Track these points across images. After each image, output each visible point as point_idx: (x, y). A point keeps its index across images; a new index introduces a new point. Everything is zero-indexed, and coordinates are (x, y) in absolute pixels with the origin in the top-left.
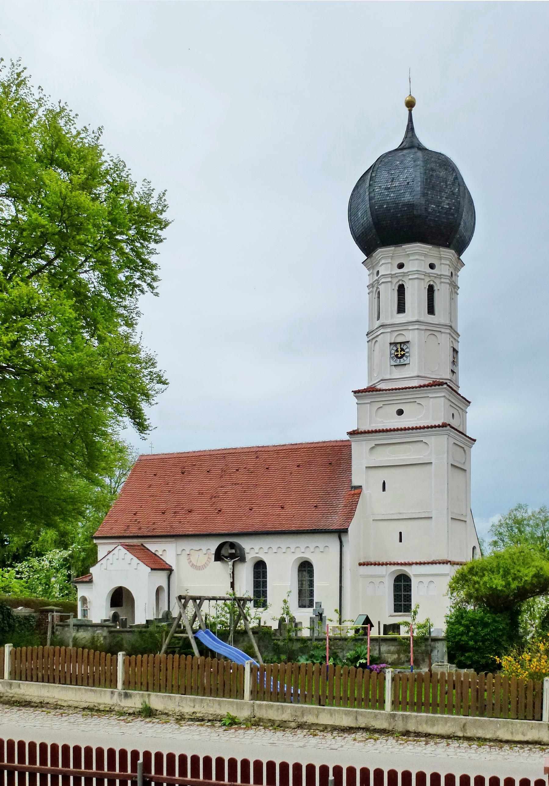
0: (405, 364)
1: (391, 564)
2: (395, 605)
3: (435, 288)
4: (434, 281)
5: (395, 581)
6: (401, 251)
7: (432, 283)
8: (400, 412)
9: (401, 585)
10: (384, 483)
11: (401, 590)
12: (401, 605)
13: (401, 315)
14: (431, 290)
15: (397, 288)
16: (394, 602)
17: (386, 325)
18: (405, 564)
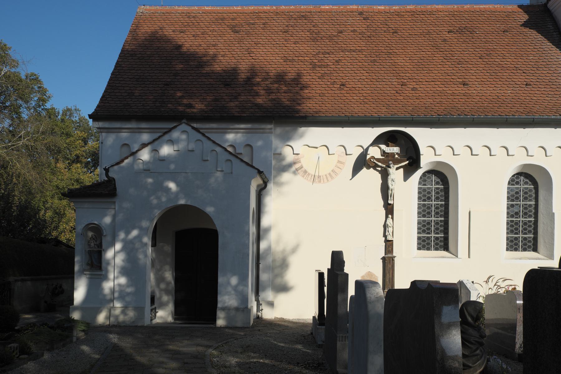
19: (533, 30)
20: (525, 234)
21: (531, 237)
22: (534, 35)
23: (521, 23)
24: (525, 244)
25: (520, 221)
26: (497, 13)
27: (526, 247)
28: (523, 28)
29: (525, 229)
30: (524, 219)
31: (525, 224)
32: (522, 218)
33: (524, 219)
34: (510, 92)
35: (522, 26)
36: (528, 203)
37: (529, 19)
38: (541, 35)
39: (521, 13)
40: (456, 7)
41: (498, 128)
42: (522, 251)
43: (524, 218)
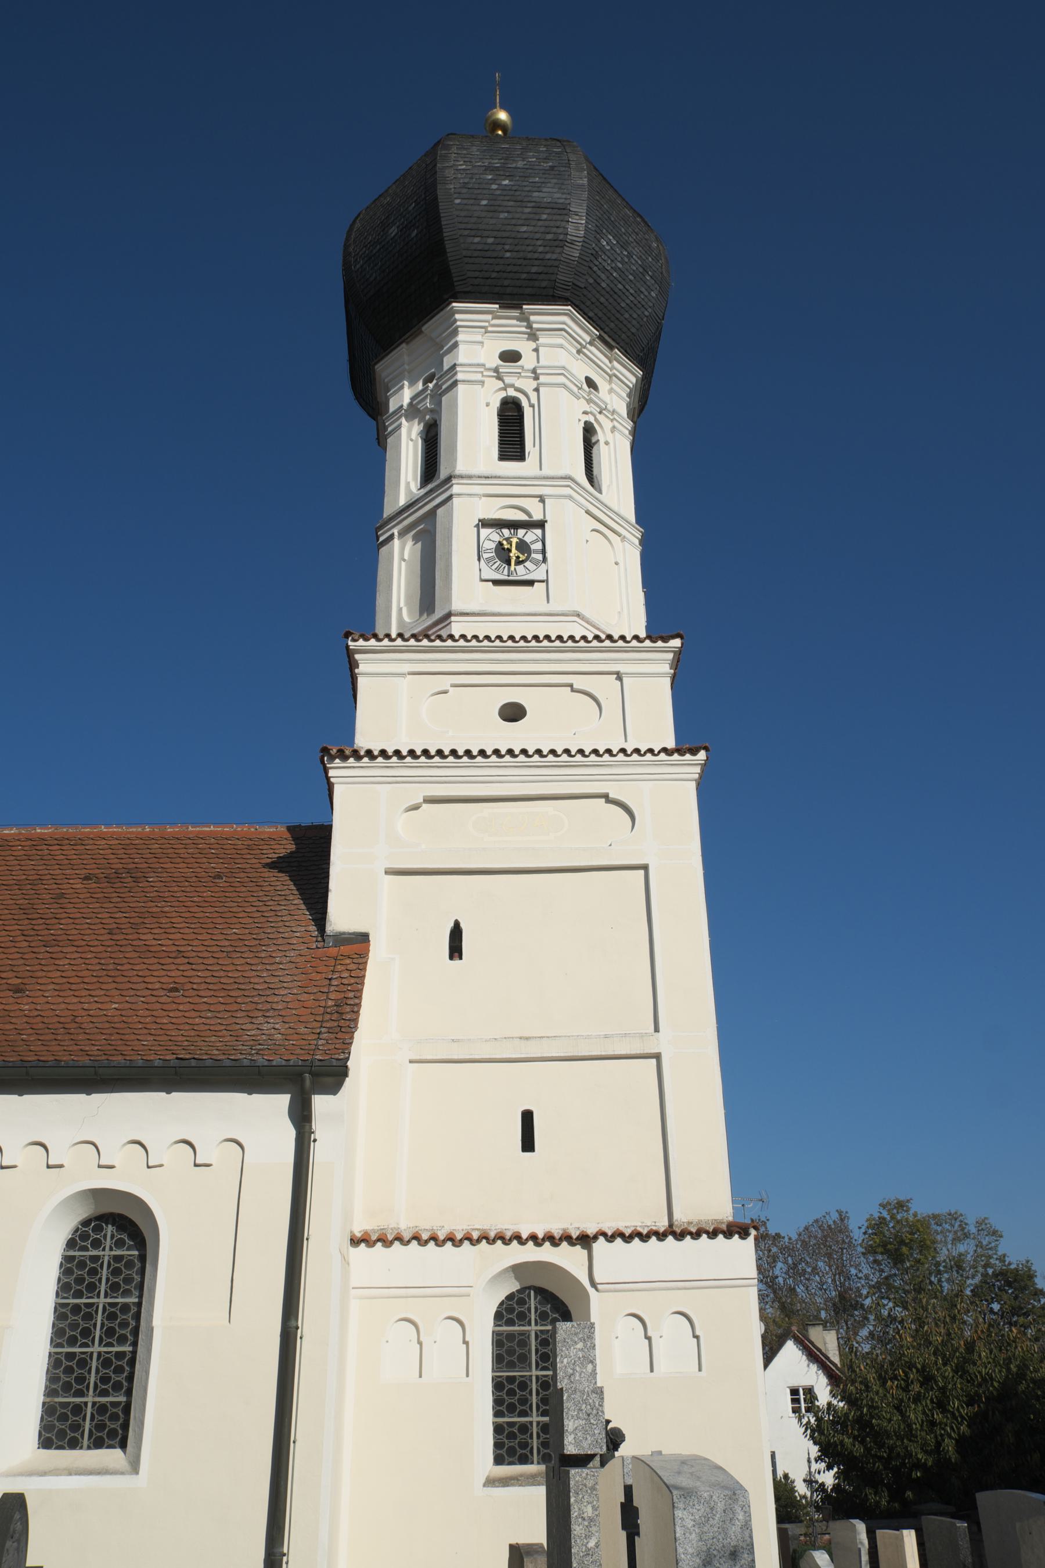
0: (530, 583)
1: (502, 1238)
2: (498, 1429)
3: (601, 436)
4: (596, 420)
5: (498, 1316)
6: (514, 322)
7: (591, 419)
8: (513, 713)
9: (525, 1335)
10: (456, 934)
11: (524, 1359)
12: (525, 1428)
13: (511, 468)
14: (589, 431)
15: (498, 404)
16: (497, 1414)
17: (470, 477)
18: (553, 1240)
19: (283, 875)
20: (104, 1393)
21: (119, 1403)
22: (283, 884)
23: (269, 861)
24: (100, 1427)
25: (92, 1353)
26: (229, 842)
27: (104, 1434)
28: (266, 870)
29: (105, 1380)
30: (106, 1349)
31: (106, 1363)
32: (100, 1345)
33: (106, 1349)
34: (116, 1006)
35: (273, 865)
36: (120, 1300)
37: (291, 853)
38: (294, 884)
39: (284, 842)
40: (148, 830)
41: (21, 1095)
42: (89, 1448)
43: (105, 1346)
